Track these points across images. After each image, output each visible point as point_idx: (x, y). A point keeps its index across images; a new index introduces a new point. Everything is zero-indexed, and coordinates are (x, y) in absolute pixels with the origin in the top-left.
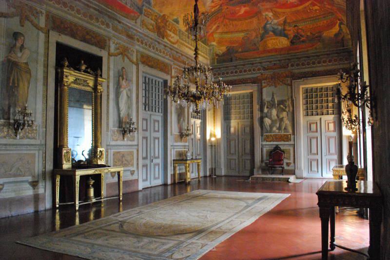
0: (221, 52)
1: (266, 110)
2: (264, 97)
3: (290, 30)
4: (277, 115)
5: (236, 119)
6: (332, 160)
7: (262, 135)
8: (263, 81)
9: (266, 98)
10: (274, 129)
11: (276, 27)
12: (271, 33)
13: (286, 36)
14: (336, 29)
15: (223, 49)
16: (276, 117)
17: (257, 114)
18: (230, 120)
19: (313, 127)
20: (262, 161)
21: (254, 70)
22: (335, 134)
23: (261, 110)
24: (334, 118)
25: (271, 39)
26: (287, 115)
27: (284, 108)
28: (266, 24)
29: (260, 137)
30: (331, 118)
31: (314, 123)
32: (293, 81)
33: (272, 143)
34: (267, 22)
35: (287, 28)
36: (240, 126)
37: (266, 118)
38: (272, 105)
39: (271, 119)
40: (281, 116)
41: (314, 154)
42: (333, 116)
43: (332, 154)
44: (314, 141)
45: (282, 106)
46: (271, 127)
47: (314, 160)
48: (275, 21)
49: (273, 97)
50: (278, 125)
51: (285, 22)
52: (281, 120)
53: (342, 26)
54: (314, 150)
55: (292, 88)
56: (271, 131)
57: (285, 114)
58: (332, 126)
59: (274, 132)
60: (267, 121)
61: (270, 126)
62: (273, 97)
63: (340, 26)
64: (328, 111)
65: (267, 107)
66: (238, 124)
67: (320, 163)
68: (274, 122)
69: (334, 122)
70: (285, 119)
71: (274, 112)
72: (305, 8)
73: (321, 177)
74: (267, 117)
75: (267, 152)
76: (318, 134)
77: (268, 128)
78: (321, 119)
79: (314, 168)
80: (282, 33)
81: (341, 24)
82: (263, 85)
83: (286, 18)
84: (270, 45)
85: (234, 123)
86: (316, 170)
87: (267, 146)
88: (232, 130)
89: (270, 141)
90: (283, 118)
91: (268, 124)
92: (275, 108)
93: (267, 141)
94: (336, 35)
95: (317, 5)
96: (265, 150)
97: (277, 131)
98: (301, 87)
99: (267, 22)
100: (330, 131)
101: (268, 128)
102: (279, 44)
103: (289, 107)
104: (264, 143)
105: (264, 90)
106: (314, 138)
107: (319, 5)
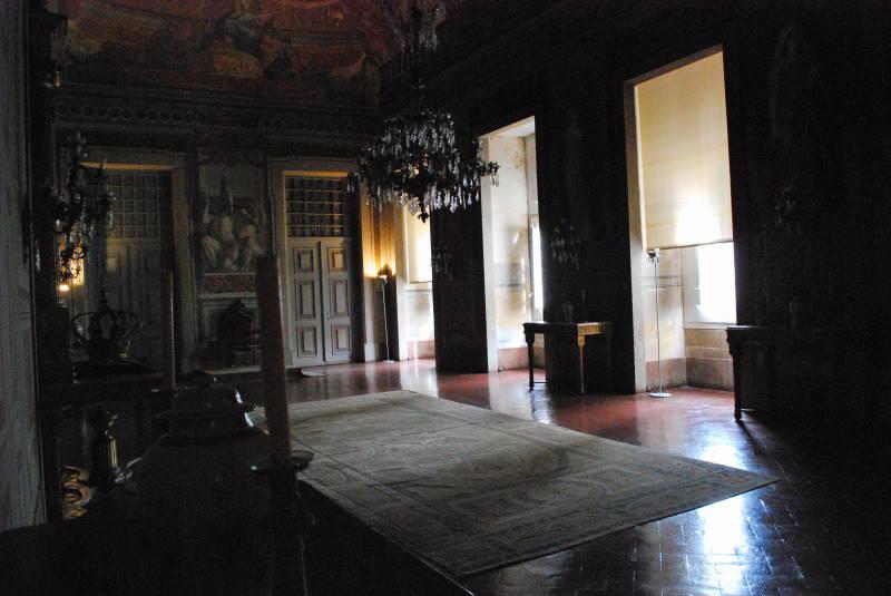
0: (82, 49)
1: (207, 218)
2: (203, 184)
3: (271, 46)
4: (235, 232)
5: (121, 237)
6: (342, 327)
7: (199, 277)
8: (200, 149)
9: (208, 187)
10: (228, 263)
11: (244, 29)
12: (229, 40)
13: (259, 54)
14: (354, 69)
15: (96, 45)
16: (232, 237)
17: (183, 226)
18: (106, 237)
19: (306, 260)
20: (201, 338)
21: (176, 117)
22: (345, 276)
23: (196, 216)
24: (343, 244)
25: (226, 53)
26: (258, 231)
27: (250, 216)
28: (227, 16)
29: (195, 281)
30: (337, 243)
31: (304, 252)
32: (269, 159)
33: (223, 295)
34: (230, 12)
35: (267, 39)
36: (133, 255)
37: (208, 237)
38: (221, 207)
39: (219, 239)
40: (243, 234)
41: (308, 317)
42: (341, 239)
43: (342, 315)
44: (307, 290)
45: (244, 212)
46: (221, 257)
47: (308, 329)
48: (249, 16)
49: (223, 190)
50: (236, 255)
51: (268, 25)
52: (244, 243)
53: (368, 66)
54: (308, 310)
55: (265, 174)
56: (219, 267)
57: (251, 230)
58: (339, 259)
59: (229, 270)
60: (211, 244)
61: (218, 256)
62: (223, 190)
63: (364, 68)
64: (333, 229)
65: (211, 212)
66: (128, 248)
67: (319, 335)
68: (226, 246)
69: (343, 252)
70: (252, 241)
71: (227, 224)
72: (320, 9)
73: (321, 361)
74: (209, 234)
75: (213, 315)
76: (315, 276)
77: (213, 258)
78: (319, 244)
79: (309, 347)
80: (255, 48)
81: (369, 60)
82: (201, 157)
83: (273, 16)
84: (218, 67)
85: (115, 248)
86: (312, 349)
87: (212, 303)
88: (111, 263)
89: (220, 292)
90: (247, 238)
91: (212, 251)
92: (229, 215)
93: (211, 291)
94: (354, 79)
95: (342, 11)
96: (206, 311)
97: (235, 267)
98: (286, 173)
99: (230, 12)
100: (337, 270)
101: (213, 258)
102: (239, 69)
103: (261, 217)
104: (204, 296)
105: (203, 169)
106: (306, 283)
107: (346, 12)
